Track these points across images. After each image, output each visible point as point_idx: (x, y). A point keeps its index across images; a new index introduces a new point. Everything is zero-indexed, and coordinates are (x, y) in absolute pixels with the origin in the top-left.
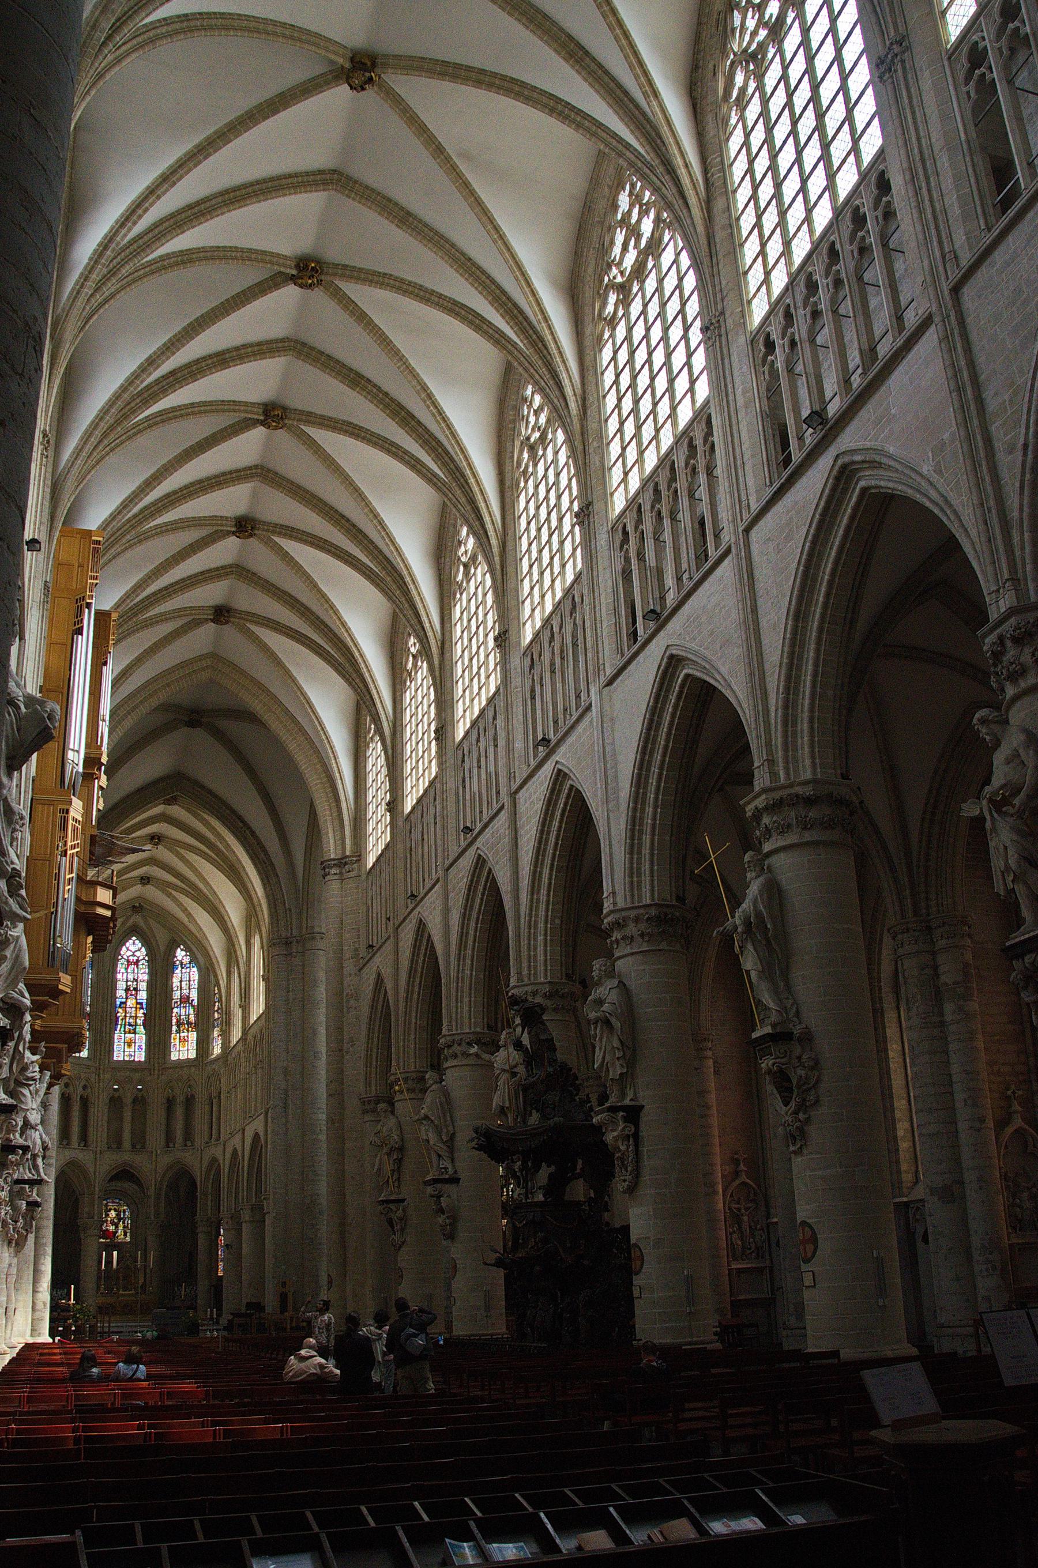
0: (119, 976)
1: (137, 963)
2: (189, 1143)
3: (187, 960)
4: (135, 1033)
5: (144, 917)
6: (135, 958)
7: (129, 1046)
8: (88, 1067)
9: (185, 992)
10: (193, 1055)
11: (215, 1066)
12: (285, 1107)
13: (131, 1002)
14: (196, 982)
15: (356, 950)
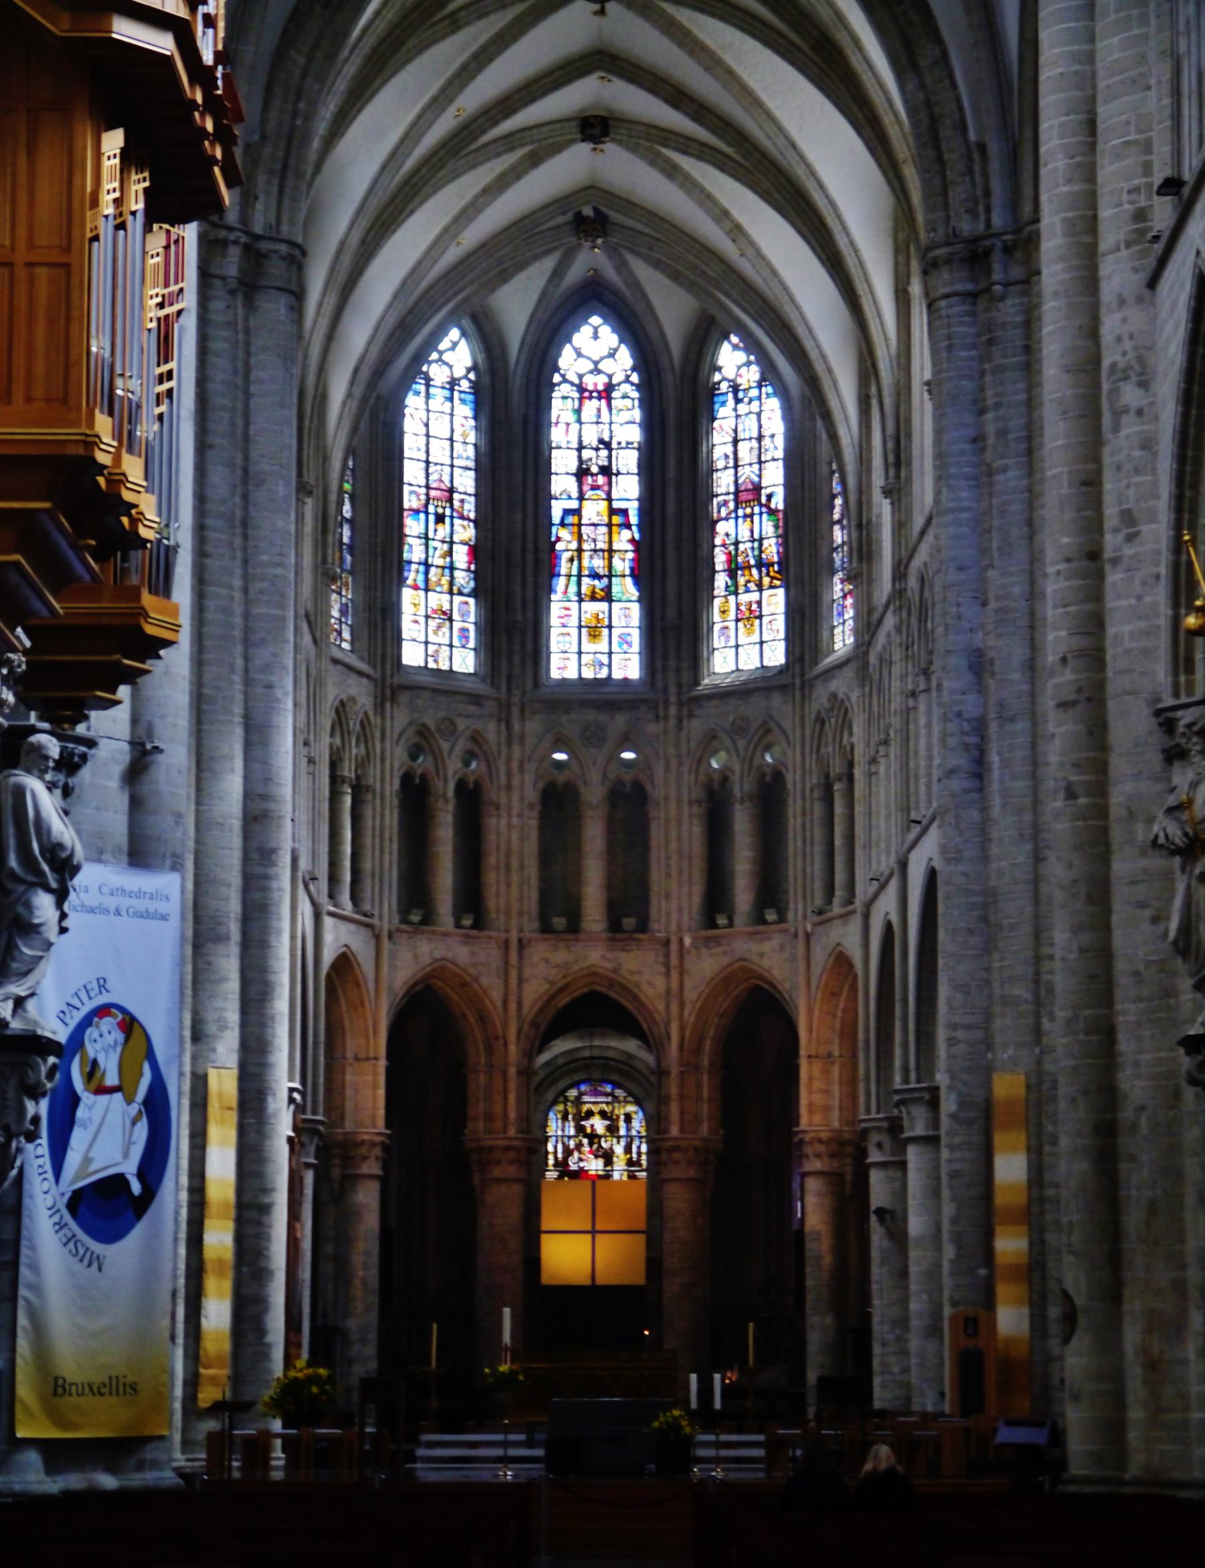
0: (557, 435)
1: (606, 393)
2: (771, 916)
3: (752, 374)
4: (608, 597)
5: (613, 251)
6: (601, 381)
7: (594, 635)
8: (475, 699)
9: (748, 473)
10: (776, 656)
11: (840, 685)
12: (979, 770)
13: (594, 510)
14: (780, 441)
15: (1141, 215)
